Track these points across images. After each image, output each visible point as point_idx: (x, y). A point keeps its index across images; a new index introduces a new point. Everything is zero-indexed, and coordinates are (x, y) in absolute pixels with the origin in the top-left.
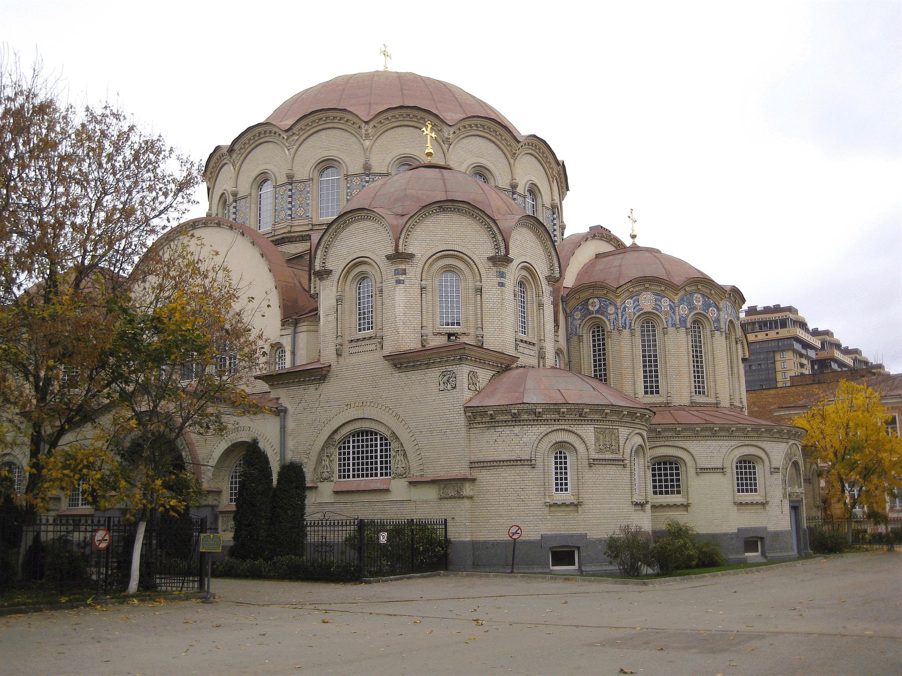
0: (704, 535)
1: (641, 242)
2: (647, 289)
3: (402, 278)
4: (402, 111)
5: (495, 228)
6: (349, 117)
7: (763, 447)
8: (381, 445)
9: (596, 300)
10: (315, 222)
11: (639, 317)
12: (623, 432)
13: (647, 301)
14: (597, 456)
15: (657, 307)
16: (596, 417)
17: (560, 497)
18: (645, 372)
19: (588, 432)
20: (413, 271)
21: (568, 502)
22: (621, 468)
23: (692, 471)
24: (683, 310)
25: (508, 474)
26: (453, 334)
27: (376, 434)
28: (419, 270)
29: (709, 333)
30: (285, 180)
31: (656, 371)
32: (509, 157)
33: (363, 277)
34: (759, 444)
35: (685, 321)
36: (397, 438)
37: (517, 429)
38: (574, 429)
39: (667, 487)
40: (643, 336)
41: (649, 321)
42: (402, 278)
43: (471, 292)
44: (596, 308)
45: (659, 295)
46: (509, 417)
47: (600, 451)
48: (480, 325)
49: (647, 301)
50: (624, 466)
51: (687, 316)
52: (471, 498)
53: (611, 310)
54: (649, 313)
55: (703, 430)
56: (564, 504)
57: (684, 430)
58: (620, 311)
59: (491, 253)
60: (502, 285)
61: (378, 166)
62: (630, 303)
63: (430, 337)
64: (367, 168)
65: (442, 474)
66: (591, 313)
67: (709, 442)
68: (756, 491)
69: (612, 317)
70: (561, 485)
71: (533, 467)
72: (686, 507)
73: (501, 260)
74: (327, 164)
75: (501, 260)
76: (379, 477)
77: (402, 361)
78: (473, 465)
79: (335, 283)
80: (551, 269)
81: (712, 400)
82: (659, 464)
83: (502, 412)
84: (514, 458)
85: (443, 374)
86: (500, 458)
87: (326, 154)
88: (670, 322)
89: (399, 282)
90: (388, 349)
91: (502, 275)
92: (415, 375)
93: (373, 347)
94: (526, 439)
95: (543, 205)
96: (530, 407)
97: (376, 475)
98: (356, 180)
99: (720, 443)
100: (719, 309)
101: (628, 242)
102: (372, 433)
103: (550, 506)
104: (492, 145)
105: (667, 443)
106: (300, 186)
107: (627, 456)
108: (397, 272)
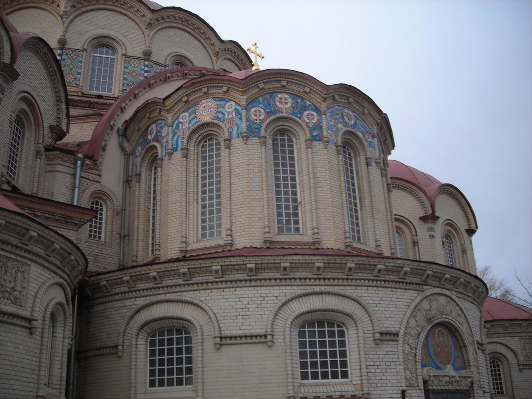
7: (354, 296)
11: (194, 132)
29: (303, 146)
34: (349, 291)
35: (259, 129)
39: (170, 372)
41: (206, 134)
44: (153, 135)
51: (263, 121)
54: (207, 124)
68: (345, 375)
81: (308, 239)
82: (161, 334)
99: (264, 291)
105: (169, 296)
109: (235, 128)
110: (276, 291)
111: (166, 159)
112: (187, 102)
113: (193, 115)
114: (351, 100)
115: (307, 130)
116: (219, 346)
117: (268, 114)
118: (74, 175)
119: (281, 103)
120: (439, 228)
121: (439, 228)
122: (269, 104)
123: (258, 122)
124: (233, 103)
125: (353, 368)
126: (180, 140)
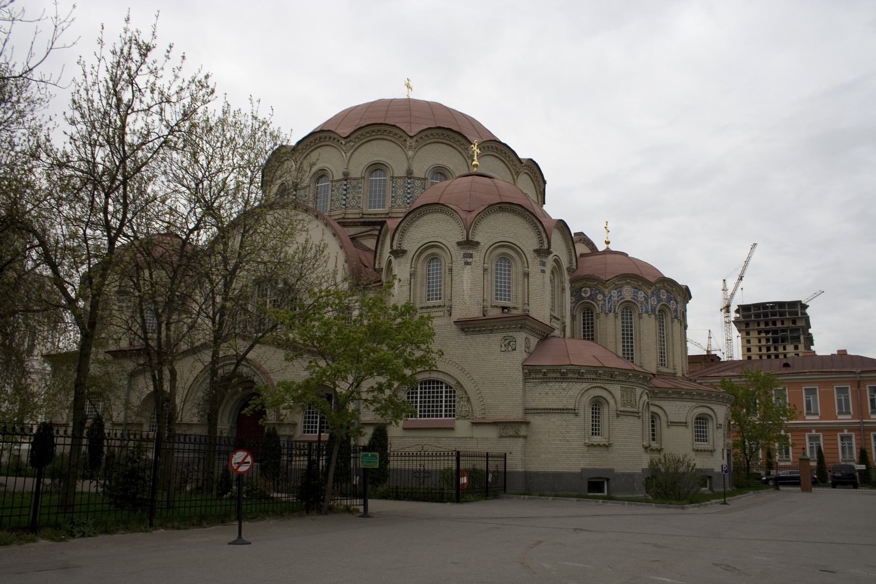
1: (613, 247)
2: (628, 283)
3: (469, 260)
4: (440, 131)
5: (540, 227)
6: (397, 131)
8: (446, 392)
10: (365, 212)
12: (639, 391)
13: (628, 293)
14: (622, 409)
15: (635, 297)
16: (622, 378)
17: (596, 440)
18: (624, 346)
19: (616, 389)
20: (478, 256)
21: (602, 444)
22: (637, 419)
23: (664, 425)
24: (653, 301)
25: (556, 419)
26: (506, 308)
27: (442, 383)
28: (483, 255)
30: (341, 177)
31: (632, 346)
33: (434, 258)
34: (710, 405)
35: (655, 309)
36: (462, 386)
37: (564, 385)
38: (607, 387)
40: (623, 319)
41: (628, 308)
42: (469, 260)
43: (520, 275)
45: (637, 288)
46: (558, 375)
47: (624, 405)
49: (628, 293)
50: (639, 417)
51: (656, 305)
52: (525, 437)
53: (600, 297)
54: (629, 301)
55: (673, 393)
56: (599, 445)
57: (660, 392)
58: (607, 299)
59: (537, 247)
60: (543, 271)
61: (417, 173)
62: (615, 293)
63: (489, 309)
64: (409, 174)
65: (501, 417)
66: (583, 298)
67: (677, 403)
69: (601, 303)
70: (595, 431)
71: (576, 415)
73: (543, 252)
74: (377, 167)
75: (543, 252)
76: (443, 418)
77: (467, 326)
78: (527, 411)
79: (409, 261)
80: (570, 262)
83: (554, 371)
84: (561, 407)
85: (505, 339)
86: (550, 407)
87: (376, 159)
89: (467, 263)
90: (457, 315)
91: (543, 264)
92: (480, 338)
93: (442, 314)
94: (571, 393)
96: (577, 368)
97: (441, 416)
98: (400, 182)
99: (685, 403)
100: (677, 303)
101: (601, 247)
102: (438, 382)
103: (589, 446)
104: (502, 164)
106: (354, 183)
107: (641, 410)
108: (466, 256)
111: (603, 315)
125: (710, 438)
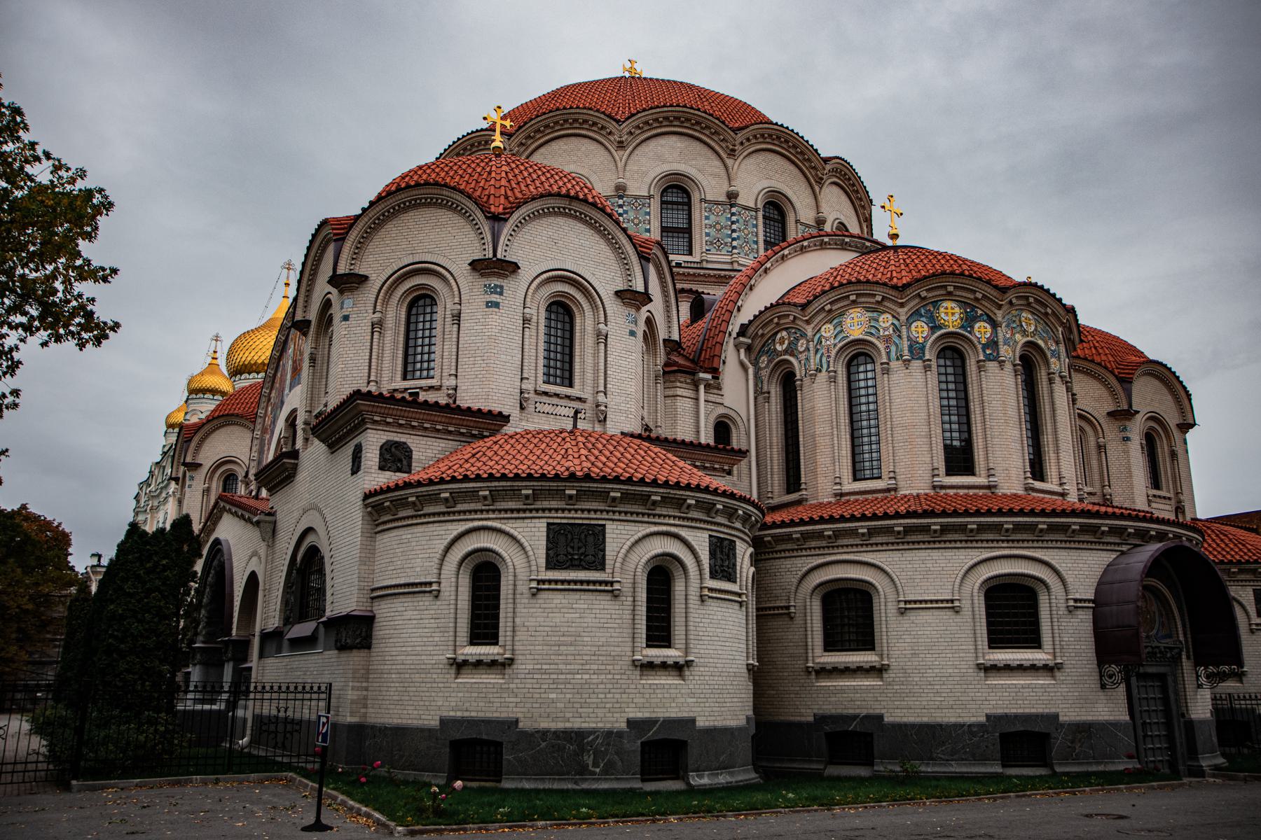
0: (913, 726)
7: (1046, 558)
9: (784, 333)
13: (856, 324)
15: (873, 328)
32: (724, 156)
35: (923, 349)
41: (858, 355)
44: (785, 346)
48: (602, 389)
49: (856, 324)
62: (828, 330)
66: (779, 354)
72: (877, 671)
88: (893, 355)
95: (797, 221)
100: (995, 325)
109: (893, 348)
110: (962, 554)
111: (807, 381)
112: (830, 311)
113: (839, 329)
114: (1031, 300)
115: (979, 347)
116: (902, 612)
117: (934, 329)
118: (697, 399)
119: (947, 314)
120: (1136, 429)
121: (1136, 429)
122: (932, 316)
123: (921, 340)
124: (890, 317)
126: (824, 360)
